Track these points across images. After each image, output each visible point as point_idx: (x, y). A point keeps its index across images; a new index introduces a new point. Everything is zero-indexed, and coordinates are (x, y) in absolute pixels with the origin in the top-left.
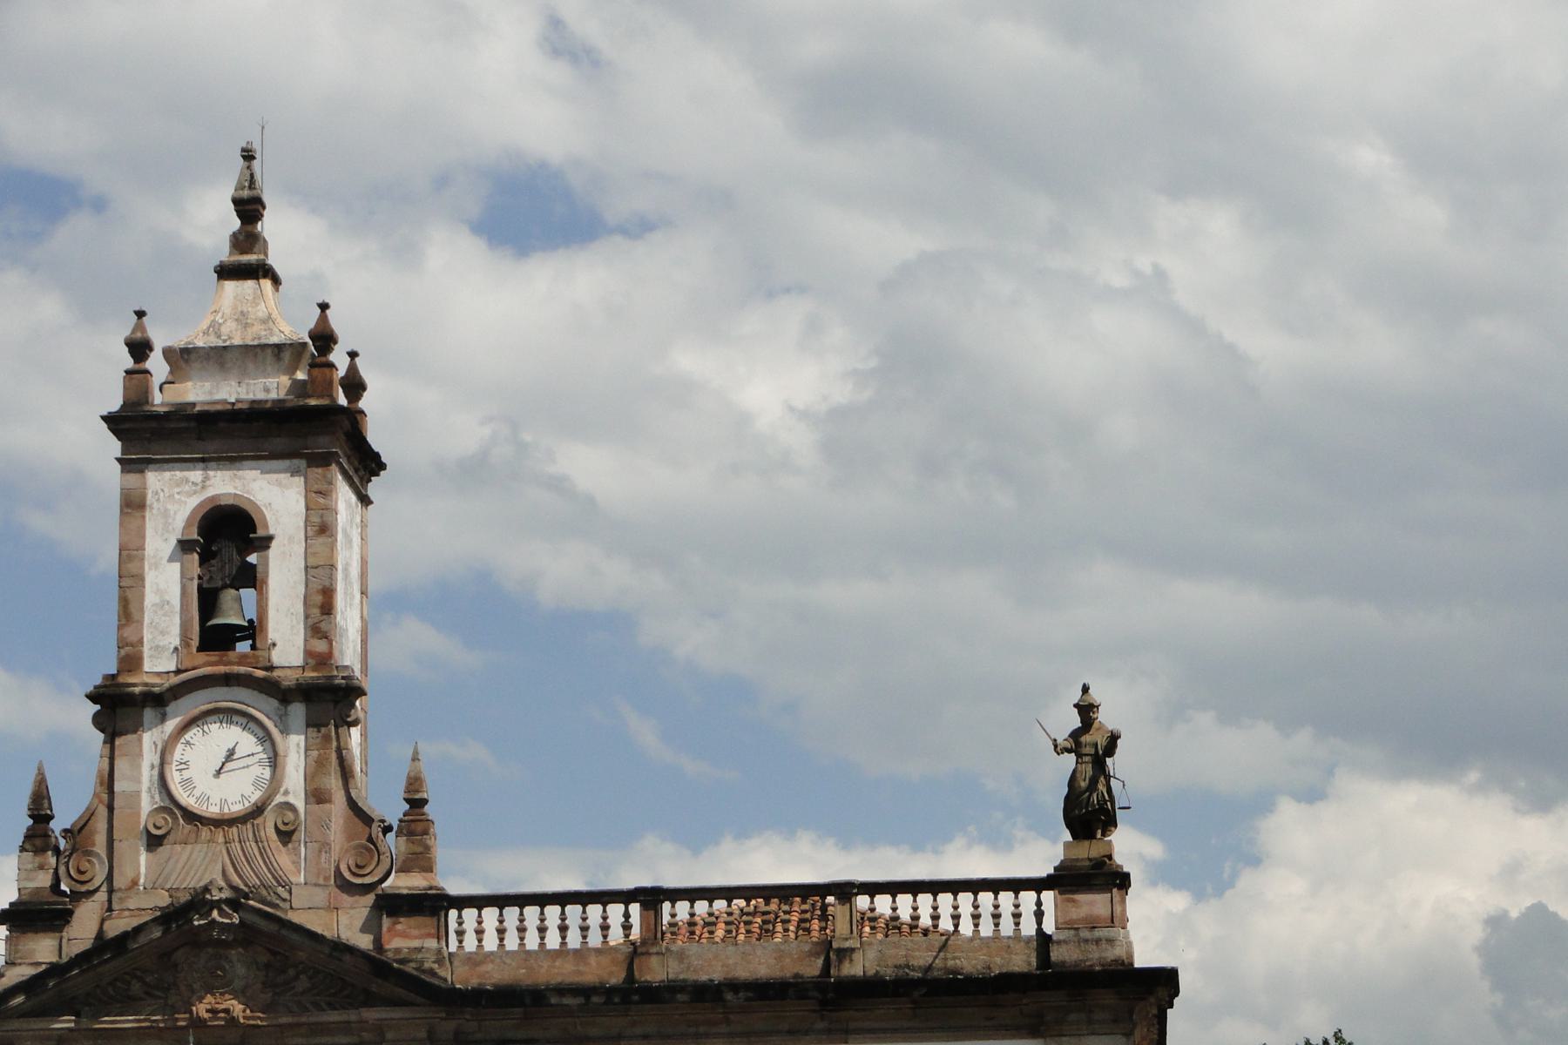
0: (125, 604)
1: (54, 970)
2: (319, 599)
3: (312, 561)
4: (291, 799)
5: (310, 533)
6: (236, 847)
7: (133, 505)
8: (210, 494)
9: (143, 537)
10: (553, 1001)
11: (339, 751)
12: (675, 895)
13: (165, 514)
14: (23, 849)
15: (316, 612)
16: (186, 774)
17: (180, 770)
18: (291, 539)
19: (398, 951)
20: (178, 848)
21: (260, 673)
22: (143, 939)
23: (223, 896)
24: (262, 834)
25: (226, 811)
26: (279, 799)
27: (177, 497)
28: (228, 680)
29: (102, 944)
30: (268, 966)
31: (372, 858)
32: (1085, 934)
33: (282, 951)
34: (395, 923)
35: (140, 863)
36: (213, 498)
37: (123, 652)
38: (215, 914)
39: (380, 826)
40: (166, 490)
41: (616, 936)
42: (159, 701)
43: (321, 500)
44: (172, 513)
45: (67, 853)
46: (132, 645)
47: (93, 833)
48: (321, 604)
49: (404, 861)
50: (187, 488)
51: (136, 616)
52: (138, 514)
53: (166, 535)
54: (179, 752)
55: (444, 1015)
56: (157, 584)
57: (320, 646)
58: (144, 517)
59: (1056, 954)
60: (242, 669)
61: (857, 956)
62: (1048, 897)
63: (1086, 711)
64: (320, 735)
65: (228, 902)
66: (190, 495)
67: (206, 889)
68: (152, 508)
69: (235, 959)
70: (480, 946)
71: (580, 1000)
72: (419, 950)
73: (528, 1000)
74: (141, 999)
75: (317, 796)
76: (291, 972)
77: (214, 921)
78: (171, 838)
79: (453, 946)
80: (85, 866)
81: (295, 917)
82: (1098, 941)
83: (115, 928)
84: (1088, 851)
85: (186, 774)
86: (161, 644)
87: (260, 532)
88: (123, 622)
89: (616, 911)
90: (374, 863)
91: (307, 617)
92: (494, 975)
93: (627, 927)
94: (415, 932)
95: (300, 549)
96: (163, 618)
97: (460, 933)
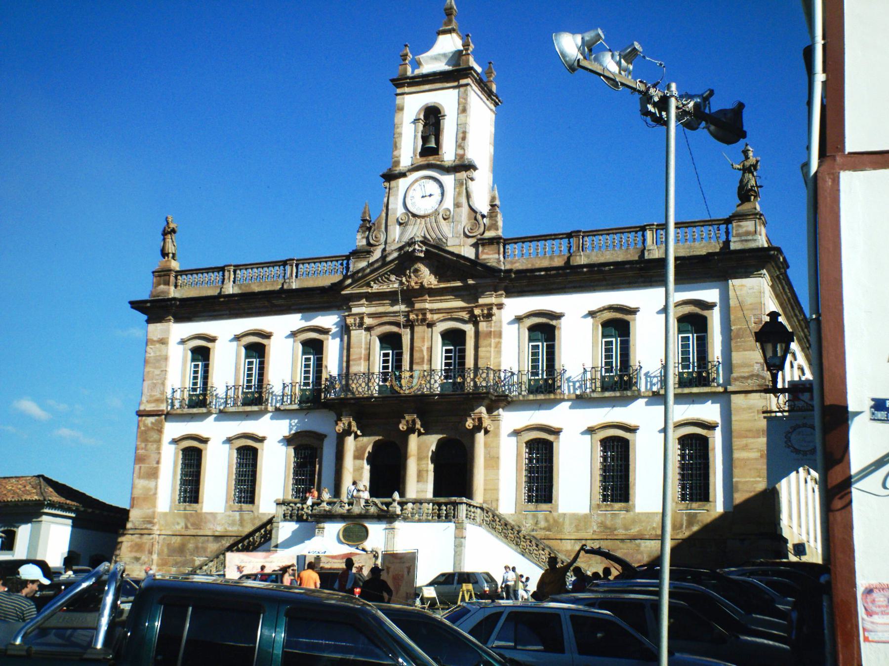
2: (461, 135)
10: (537, 274)
11: (466, 188)
15: (460, 141)
16: (413, 201)
19: (485, 259)
21: (439, 163)
31: (476, 226)
37: (393, 160)
38: (417, 247)
42: (403, 175)
46: (397, 157)
54: (410, 193)
55: (498, 281)
57: (461, 152)
65: (421, 242)
75: (457, 205)
80: (379, 236)
81: (447, 248)
87: (442, 114)
94: (491, 252)
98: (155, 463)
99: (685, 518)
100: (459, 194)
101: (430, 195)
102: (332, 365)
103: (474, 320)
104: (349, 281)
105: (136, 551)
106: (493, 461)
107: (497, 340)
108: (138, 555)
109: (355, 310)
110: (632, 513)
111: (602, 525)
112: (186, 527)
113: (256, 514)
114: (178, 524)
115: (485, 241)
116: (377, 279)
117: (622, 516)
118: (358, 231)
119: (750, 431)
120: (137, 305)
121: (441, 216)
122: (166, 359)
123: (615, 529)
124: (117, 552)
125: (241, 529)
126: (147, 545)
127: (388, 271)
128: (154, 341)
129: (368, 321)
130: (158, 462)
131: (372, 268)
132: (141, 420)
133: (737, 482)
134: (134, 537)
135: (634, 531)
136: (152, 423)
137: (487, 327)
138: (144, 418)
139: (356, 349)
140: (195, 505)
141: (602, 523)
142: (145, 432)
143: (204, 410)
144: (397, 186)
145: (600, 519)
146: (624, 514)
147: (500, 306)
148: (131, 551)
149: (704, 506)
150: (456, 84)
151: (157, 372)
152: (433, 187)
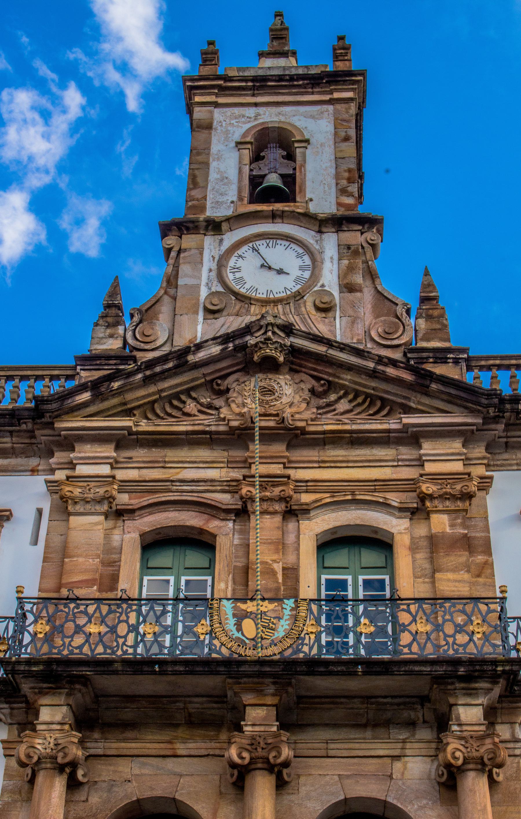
3: (339, 155)
4: (326, 288)
5: (337, 140)
8: (261, 121)
9: (210, 143)
13: (227, 132)
16: (238, 275)
17: (234, 272)
20: (231, 318)
22: (202, 355)
24: (303, 309)
25: (272, 296)
27: (236, 124)
28: (274, 216)
30: (312, 391)
33: (325, 377)
36: (263, 123)
37: (190, 204)
38: (270, 334)
39: (403, 308)
40: (227, 120)
44: (231, 132)
45: (134, 324)
46: (198, 200)
47: (160, 312)
49: (424, 334)
50: (243, 119)
51: (201, 183)
52: (206, 131)
53: (226, 143)
55: (480, 421)
56: (218, 168)
58: (210, 134)
60: (286, 209)
64: (350, 251)
66: (245, 123)
68: (216, 129)
69: (283, 383)
74: (195, 415)
76: (333, 397)
77: (269, 339)
78: (224, 313)
85: (238, 275)
86: (220, 200)
88: (191, 186)
90: (400, 332)
91: (337, 184)
96: (223, 186)
100: (351, 269)
104: (86, 396)
107: (480, 558)
115: (425, 355)
118: (96, 324)
121: (310, 307)
127: (182, 392)
129: (123, 499)
131: (148, 373)
137: (452, 526)
139: (81, 560)
144: (201, 250)
150: (327, 97)
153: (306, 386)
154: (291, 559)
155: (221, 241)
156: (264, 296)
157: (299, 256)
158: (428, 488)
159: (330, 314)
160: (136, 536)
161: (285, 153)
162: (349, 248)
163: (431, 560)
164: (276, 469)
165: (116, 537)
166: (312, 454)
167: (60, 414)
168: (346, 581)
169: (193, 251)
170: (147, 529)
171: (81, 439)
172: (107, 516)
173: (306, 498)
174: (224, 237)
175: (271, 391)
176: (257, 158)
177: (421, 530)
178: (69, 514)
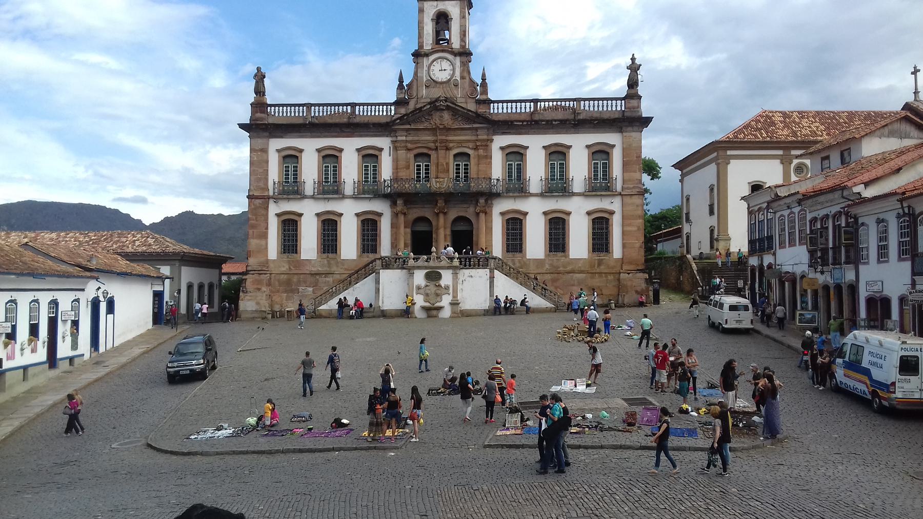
0: (419, 33)
1: (404, 115)
4: (457, 78)
6: (445, 89)
7: (421, 11)
8: (438, 8)
10: (515, 123)
12: (541, 101)
14: (397, 89)
15: (462, 36)
16: (433, 72)
18: (456, 19)
19: (480, 112)
20: (432, 89)
22: (425, 108)
23: (443, 99)
26: (454, 78)
28: (443, 51)
29: (416, 110)
30: (452, 115)
32: (632, 110)
34: (480, 106)
35: (424, 92)
41: (528, 110)
42: (427, 55)
43: (463, 10)
48: (463, 34)
51: (422, 37)
57: (463, 44)
59: (625, 114)
61: (581, 114)
62: (623, 102)
63: (633, 59)
67: (439, 97)
70: (498, 112)
71: (521, 123)
72: (485, 112)
73: (510, 123)
75: (462, 78)
76: (457, 117)
77: (441, 104)
79: (492, 112)
82: (635, 111)
83: (418, 106)
84: (633, 91)
85: (433, 72)
87: (450, 17)
89: (528, 104)
92: (501, 118)
93: (530, 108)
95: (458, 21)
97: (494, 109)
98: (264, 229)
99: (596, 262)
101: (445, 70)
102: (386, 171)
103: (476, 148)
104: (398, 121)
105: (258, 284)
106: (489, 230)
107: (489, 160)
108: (259, 287)
109: (399, 138)
110: (567, 259)
111: (551, 265)
112: (290, 268)
113: (339, 260)
114: (284, 267)
116: (414, 120)
117: (562, 261)
119: (633, 216)
120: (242, 126)
122: (267, 162)
123: (559, 268)
124: (244, 285)
125: (328, 269)
126: (264, 281)
128: (257, 150)
129: (409, 145)
130: (267, 228)
132: (251, 202)
133: (625, 243)
134: (254, 275)
135: (569, 268)
136: (260, 204)
138: (253, 200)
139: (401, 162)
140: (295, 255)
141: (551, 264)
142: (255, 209)
143: (299, 197)
145: (550, 263)
146: (564, 259)
147: (492, 141)
148: (253, 285)
149: (606, 255)
151: (261, 170)
152: (446, 65)
153: (451, 114)
154: (447, 161)
155: (429, 59)
156: (440, 80)
157: (450, 66)
158: (478, 144)
159: (457, 87)
160: (412, 155)
161: (445, 21)
162: (463, 63)
163: (478, 161)
164: (444, 138)
165: (408, 155)
166: (452, 132)
167: (393, 125)
168: (460, 164)
169: (421, 64)
170: (415, 153)
171: (399, 130)
172: (405, 150)
173: (451, 145)
174: (430, 57)
175: (442, 117)
176: (437, 23)
177: (476, 153)
178: (397, 150)
